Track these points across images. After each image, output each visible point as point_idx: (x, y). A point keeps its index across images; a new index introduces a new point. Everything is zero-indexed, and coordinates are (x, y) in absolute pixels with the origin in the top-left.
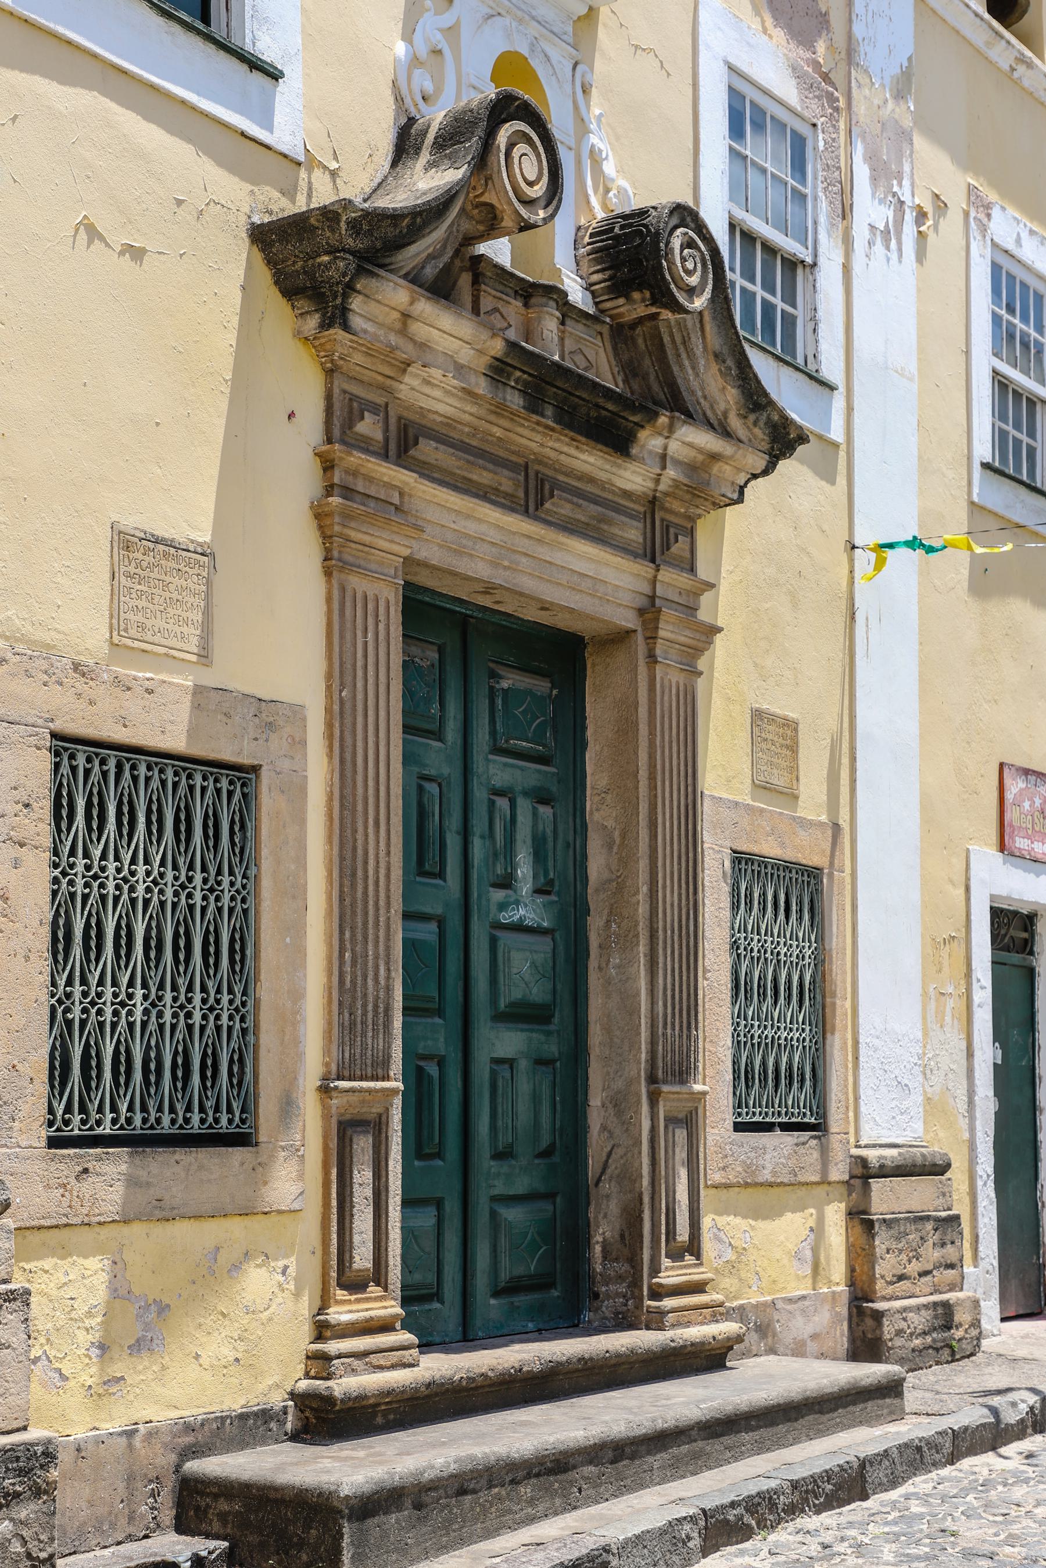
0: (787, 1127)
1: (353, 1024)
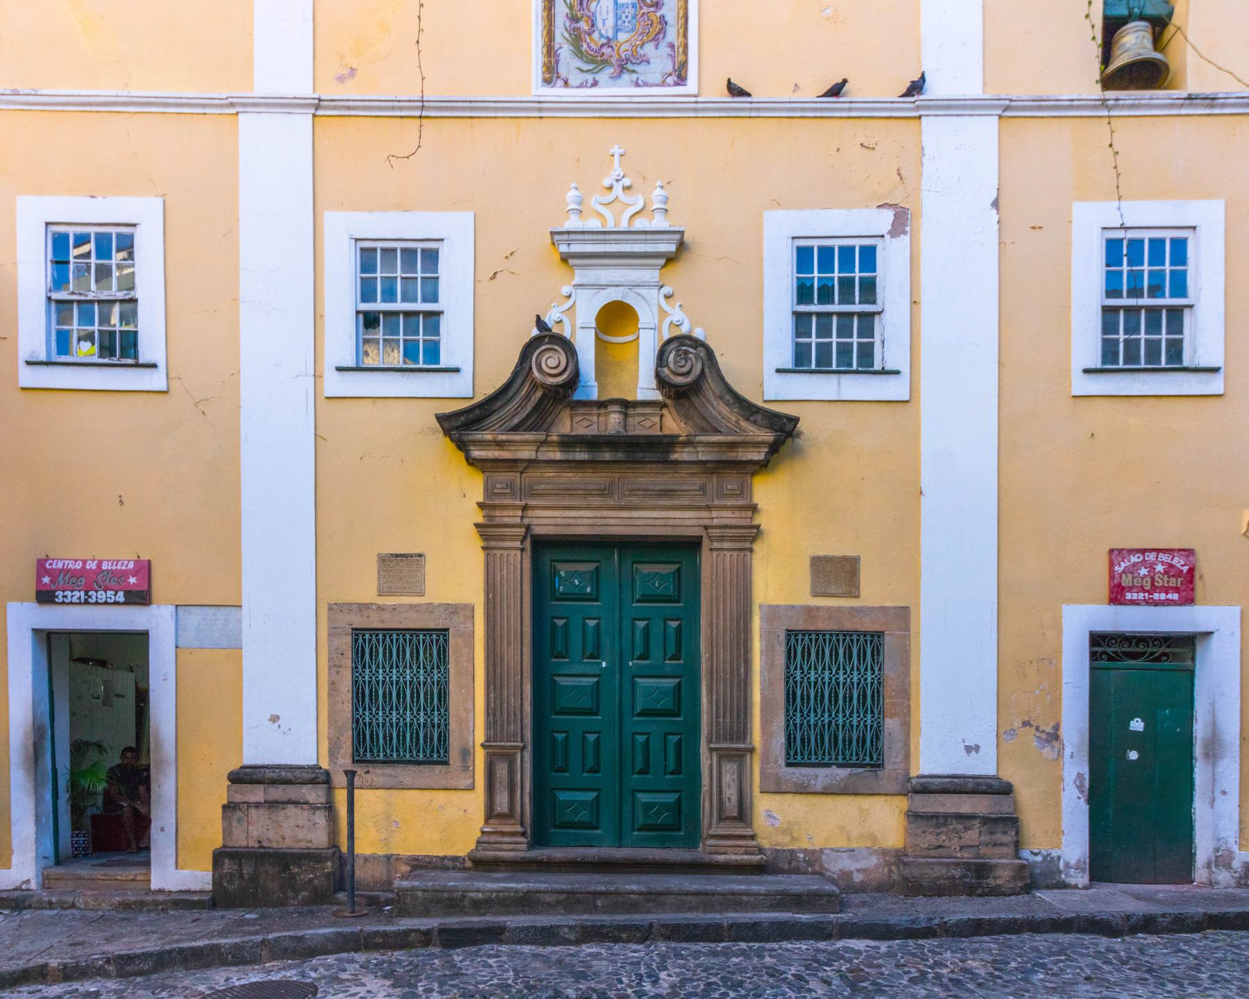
0: (839, 766)
1: (495, 722)
